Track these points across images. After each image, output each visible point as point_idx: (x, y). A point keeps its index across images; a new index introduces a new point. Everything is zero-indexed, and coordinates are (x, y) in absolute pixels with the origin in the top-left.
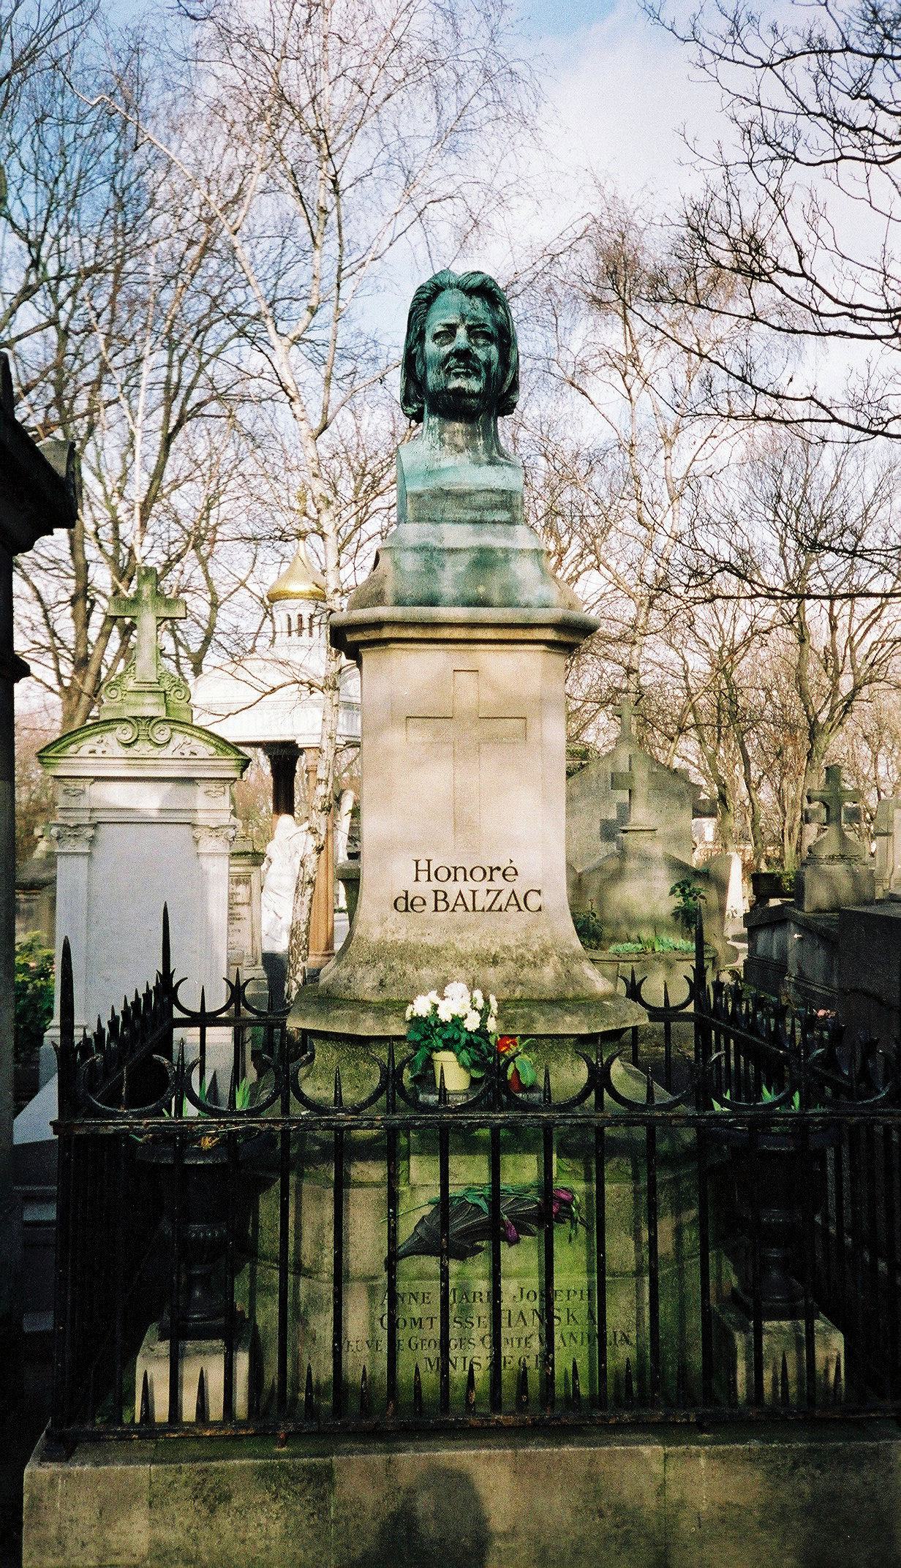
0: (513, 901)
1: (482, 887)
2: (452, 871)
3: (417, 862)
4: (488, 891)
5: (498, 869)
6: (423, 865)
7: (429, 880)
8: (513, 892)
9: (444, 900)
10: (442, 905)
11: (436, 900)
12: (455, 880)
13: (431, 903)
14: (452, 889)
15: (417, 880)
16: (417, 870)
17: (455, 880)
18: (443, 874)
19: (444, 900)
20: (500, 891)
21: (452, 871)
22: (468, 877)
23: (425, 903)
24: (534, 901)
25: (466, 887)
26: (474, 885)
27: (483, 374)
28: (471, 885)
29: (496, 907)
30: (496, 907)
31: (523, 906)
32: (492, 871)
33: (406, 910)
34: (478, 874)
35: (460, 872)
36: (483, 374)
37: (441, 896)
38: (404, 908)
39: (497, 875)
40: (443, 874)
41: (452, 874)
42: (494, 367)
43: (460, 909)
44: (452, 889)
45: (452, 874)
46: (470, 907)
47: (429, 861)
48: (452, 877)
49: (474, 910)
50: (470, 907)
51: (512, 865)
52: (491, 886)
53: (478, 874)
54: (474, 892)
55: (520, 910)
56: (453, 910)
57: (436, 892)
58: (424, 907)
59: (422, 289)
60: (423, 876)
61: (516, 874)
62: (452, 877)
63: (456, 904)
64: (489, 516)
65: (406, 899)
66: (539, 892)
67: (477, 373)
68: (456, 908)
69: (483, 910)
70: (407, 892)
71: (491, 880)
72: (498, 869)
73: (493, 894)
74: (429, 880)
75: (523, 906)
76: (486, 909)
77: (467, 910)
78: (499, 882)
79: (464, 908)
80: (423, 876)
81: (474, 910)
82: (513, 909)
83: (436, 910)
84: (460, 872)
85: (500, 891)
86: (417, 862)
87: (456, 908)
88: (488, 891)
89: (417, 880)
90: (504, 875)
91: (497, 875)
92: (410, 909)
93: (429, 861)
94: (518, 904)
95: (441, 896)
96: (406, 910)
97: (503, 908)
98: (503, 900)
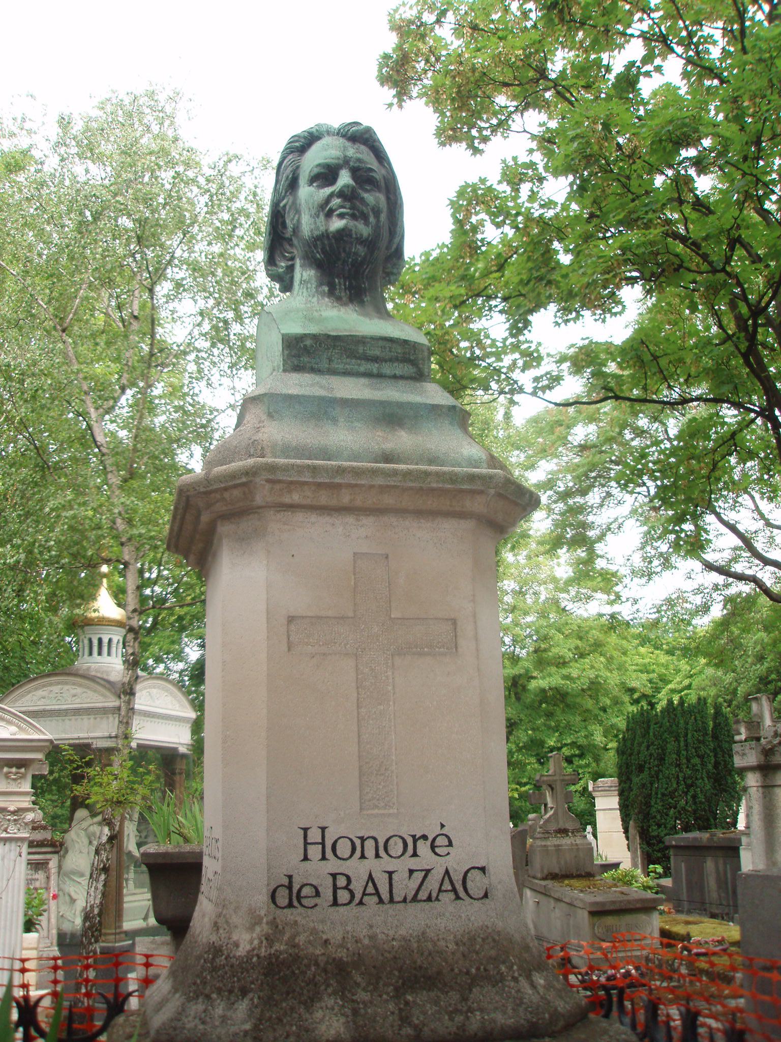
0: (447, 886)
1: (402, 866)
2: (358, 843)
3: (305, 830)
5: (425, 837)
7: (324, 858)
8: (447, 872)
9: (346, 888)
10: (343, 896)
11: (335, 888)
12: (363, 856)
13: (327, 893)
15: (306, 858)
16: (306, 844)
17: (363, 856)
18: (344, 849)
19: (346, 888)
20: (428, 872)
21: (358, 843)
22: (382, 852)
23: (318, 894)
24: (476, 883)
27: (372, 219)
28: (387, 863)
29: (423, 895)
30: (423, 895)
31: (462, 893)
32: (415, 840)
33: (290, 905)
34: (396, 847)
35: (370, 844)
37: (342, 882)
38: (286, 901)
39: (423, 848)
40: (344, 849)
43: (372, 900)
44: (358, 870)
45: (357, 848)
46: (385, 896)
47: (323, 829)
48: (358, 853)
49: (392, 900)
50: (385, 896)
51: (445, 831)
52: (413, 863)
53: (396, 847)
54: (390, 874)
55: (458, 897)
56: (361, 903)
57: (334, 876)
58: (317, 900)
59: (295, 139)
60: (315, 852)
61: (450, 844)
62: (358, 853)
63: (364, 894)
64: (387, 369)
65: (290, 887)
66: (483, 869)
67: (365, 217)
69: (405, 900)
70: (290, 877)
71: (415, 855)
72: (425, 837)
73: (419, 876)
74: (324, 858)
75: (462, 893)
76: (409, 898)
77: (381, 901)
79: (375, 899)
80: (315, 852)
81: (392, 900)
82: (447, 897)
83: (335, 903)
84: (370, 844)
85: (428, 872)
86: (305, 830)
87: (366, 898)
88: (411, 872)
89: (306, 858)
90: (433, 847)
91: (423, 848)
92: (295, 903)
93: (323, 829)
94: (454, 890)
95: (342, 882)
96: (290, 905)
97: (434, 895)
98: (433, 884)
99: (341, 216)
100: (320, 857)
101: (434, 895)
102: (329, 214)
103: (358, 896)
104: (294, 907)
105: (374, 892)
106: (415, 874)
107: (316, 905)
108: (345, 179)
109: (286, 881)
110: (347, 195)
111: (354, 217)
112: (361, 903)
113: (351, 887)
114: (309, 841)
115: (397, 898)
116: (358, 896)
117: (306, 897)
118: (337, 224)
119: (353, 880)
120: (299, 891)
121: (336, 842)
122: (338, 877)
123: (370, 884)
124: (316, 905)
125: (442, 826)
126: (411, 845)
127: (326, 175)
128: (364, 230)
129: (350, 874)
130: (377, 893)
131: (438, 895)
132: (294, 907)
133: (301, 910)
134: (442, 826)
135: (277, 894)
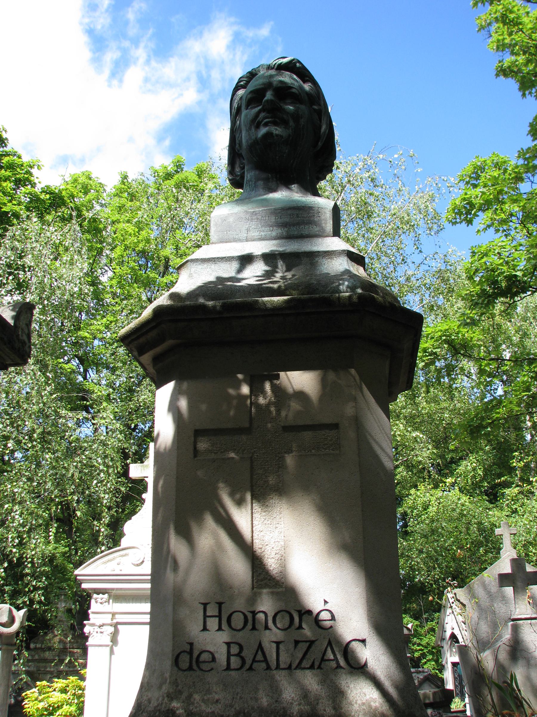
3: (205, 605)
4: (297, 642)
9: (238, 655)
12: (254, 628)
15: (205, 629)
16: (205, 616)
19: (238, 655)
21: (250, 616)
23: (214, 659)
27: (291, 123)
33: (190, 668)
36: (291, 123)
42: (302, 122)
46: (273, 664)
49: (278, 667)
50: (273, 664)
51: (328, 607)
56: (251, 668)
58: (213, 665)
62: (250, 626)
63: (254, 661)
65: (191, 653)
67: (284, 123)
68: (255, 665)
69: (289, 668)
70: (191, 644)
73: (303, 647)
76: (294, 666)
77: (268, 668)
79: (264, 665)
80: (213, 623)
83: (228, 668)
87: (255, 665)
88: (297, 642)
89: (205, 629)
92: (195, 667)
95: (235, 650)
96: (190, 668)
97: (317, 664)
99: (266, 125)
100: (217, 628)
101: (317, 664)
102: (258, 127)
103: (248, 662)
104: (194, 670)
105: (262, 659)
106: (300, 645)
107: (212, 669)
109: (188, 648)
112: (251, 668)
113: (243, 654)
114: (208, 614)
115: (282, 666)
116: (248, 662)
117: (204, 662)
118: (263, 131)
119: (244, 648)
120: (199, 656)
121: (230, 615)
122: (232, 645)
123: (260, 652)
124: (212, 669)
125: (326, 602)
129: (242, 644)
130: (266, 660)
131: (320, 664)
132: (194, 670)
133: (199, 673)
134: (326, 602)
135: (180, 659)
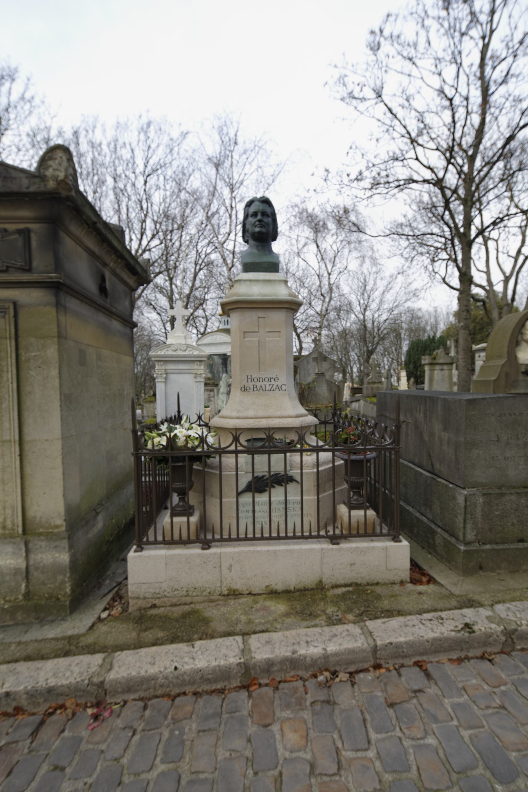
1: (267, 384)
6: (249, 377)
10: (255, 389)
13: (252, 388)
14: (258, 384)
18: (255, 380)
24: (284, 388)
25: (262, 384)
26: (266, 383)
28: (265, 383)
39: (272, 380)
40: (255, 380)
41: (258, 380)
44: (258, 384)
45: (258, 380)
53: (267, 380)
60: (249, 381)
67: (264, 226)
78: (273, 382)
80: (249, 381)
82: (277, 390)
91: (272, 380)
98: (274, 387)
102: (256, 226)
108: (259, 217)
110: (260, 221)
111: (261, 227)
126: (270, 379)
127: (255, 214)
128: (264, 230)
